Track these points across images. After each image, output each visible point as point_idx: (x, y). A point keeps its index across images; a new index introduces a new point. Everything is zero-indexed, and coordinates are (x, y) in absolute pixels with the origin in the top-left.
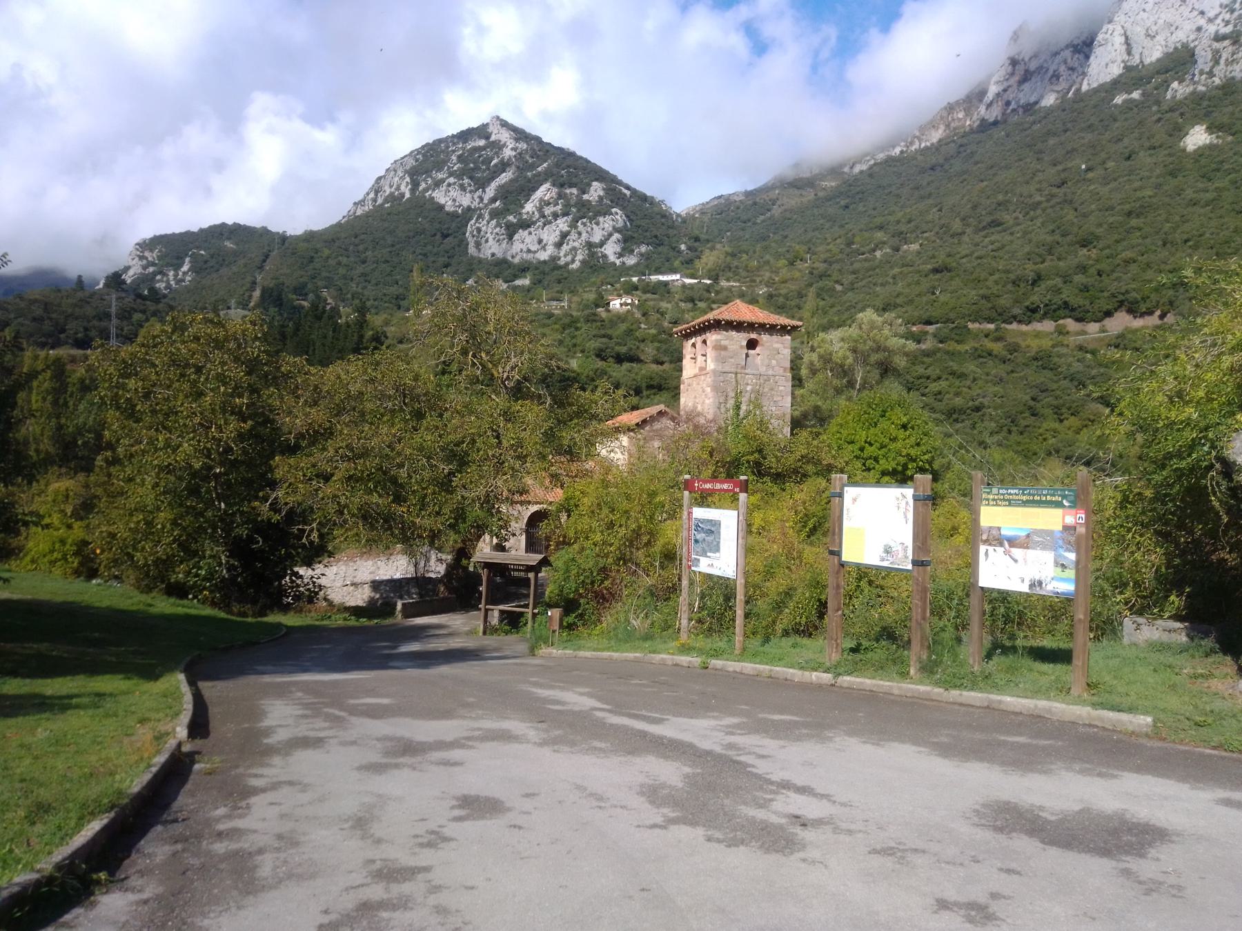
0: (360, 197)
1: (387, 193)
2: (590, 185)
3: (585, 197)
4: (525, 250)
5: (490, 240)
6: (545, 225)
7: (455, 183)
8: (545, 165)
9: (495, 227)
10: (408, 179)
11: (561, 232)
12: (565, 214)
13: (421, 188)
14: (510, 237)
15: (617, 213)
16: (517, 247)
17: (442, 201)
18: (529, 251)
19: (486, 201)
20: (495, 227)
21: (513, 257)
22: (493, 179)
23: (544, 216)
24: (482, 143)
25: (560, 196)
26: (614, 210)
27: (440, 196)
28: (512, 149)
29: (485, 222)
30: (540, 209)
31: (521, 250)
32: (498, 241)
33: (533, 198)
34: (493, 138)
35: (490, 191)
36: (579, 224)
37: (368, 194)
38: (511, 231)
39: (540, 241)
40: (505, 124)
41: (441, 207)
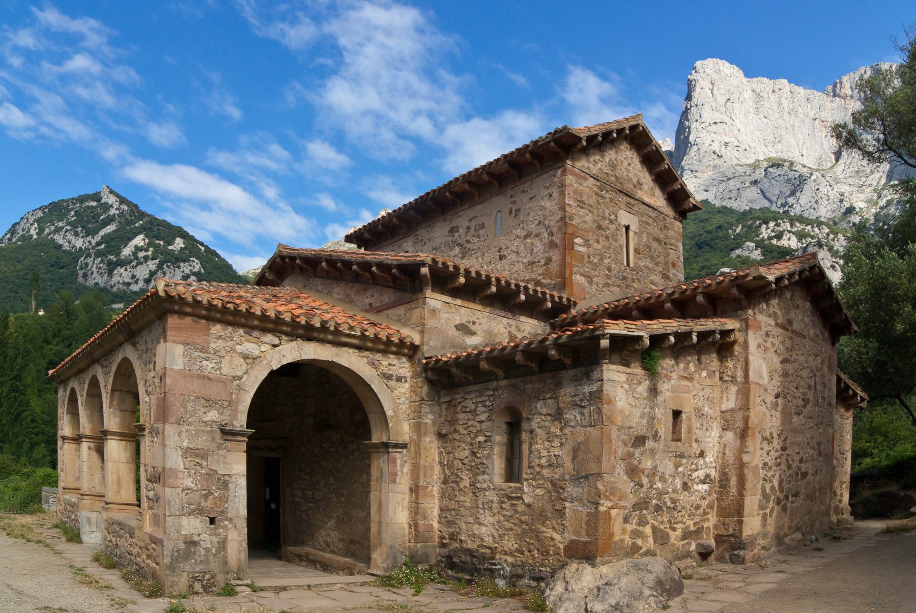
2: (174, 239)
3: (170, 247)
4: (121, 282)
5: (95, 272)
6: (138, 264)
8: (141, 222)
9: (100, 263)
11: (150, 271)
12: (153, 259)
14: (110, 273)
15: (194, 261)
16: (116, 279)
20: (100, 263)
21: (112, 287)
23: (137, 258)
25: (150, 244)
26: (192, 259)
30: (135, 254)
31: (119, 282)
36: (165, 266)
38: (111, 268)
39: (133, 277)
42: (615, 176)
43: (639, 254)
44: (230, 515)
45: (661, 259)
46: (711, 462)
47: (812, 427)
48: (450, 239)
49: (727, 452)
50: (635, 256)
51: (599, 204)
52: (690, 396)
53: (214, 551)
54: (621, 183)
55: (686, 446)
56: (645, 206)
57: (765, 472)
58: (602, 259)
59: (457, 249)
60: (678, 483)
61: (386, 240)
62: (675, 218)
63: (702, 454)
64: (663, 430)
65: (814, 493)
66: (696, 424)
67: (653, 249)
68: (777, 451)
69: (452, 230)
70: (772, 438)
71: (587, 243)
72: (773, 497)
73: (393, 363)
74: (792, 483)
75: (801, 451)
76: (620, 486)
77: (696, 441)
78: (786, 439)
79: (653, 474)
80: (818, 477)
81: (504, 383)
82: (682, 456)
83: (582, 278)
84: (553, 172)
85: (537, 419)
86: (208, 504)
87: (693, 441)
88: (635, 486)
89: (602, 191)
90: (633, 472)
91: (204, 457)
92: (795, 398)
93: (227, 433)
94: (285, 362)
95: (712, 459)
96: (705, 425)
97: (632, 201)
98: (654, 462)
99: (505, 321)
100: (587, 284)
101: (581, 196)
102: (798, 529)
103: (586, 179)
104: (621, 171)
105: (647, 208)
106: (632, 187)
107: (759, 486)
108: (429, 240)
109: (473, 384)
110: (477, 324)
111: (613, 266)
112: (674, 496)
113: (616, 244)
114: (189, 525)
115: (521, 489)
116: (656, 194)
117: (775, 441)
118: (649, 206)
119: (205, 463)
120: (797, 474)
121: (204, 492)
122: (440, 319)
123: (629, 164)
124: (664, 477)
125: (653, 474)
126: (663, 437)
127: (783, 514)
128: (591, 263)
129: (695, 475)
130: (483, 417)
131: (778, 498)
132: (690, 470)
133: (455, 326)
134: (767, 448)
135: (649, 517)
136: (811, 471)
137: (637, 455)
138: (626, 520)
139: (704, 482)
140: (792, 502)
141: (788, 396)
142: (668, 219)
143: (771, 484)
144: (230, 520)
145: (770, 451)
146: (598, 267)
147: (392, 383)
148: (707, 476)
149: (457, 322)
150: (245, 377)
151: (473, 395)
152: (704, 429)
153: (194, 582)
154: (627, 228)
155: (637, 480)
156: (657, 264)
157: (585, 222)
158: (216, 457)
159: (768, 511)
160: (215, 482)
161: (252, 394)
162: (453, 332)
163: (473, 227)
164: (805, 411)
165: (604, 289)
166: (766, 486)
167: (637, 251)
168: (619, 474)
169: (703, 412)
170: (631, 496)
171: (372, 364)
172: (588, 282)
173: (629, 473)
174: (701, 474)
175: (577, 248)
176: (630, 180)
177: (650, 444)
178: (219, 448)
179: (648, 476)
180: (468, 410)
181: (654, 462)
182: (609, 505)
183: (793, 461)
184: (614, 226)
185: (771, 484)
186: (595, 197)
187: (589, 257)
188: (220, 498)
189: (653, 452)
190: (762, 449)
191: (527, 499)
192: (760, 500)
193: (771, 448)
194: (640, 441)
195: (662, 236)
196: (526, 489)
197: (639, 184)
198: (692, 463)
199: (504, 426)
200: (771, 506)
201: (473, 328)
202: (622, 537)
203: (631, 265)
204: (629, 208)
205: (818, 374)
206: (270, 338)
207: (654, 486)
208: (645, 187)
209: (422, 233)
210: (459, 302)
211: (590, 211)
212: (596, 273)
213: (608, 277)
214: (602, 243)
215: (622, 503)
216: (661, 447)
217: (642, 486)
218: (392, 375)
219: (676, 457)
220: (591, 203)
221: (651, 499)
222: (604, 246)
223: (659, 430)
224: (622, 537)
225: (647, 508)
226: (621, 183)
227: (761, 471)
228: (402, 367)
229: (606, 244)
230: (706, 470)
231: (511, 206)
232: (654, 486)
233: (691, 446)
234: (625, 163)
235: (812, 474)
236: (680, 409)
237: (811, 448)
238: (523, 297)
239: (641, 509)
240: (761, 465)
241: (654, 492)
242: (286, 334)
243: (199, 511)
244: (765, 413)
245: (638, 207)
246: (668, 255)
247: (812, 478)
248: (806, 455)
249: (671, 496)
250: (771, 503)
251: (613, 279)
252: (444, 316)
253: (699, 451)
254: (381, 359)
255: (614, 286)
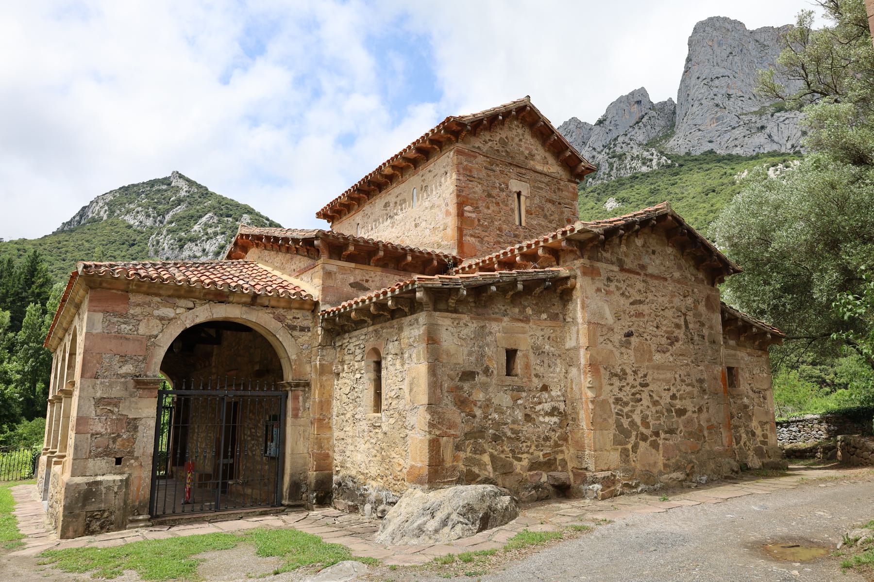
0: (68, 220)
1: (90, 217)
2: (242, 216)
4: (191, 255)
6: (208, 239)
7: (141, 211)
8: (210, 202)
9: (171, 240)
10: (106, 208)
12: (223, 233)
13: (115, 214)
16: (186, 253)
17: (132, 222)
18: (195, 257)
19: (165, 223)
22: (172, 209)
23: (207, 234)
24: (164, 187)
25: (219, 222)
27: (130, 220)
28: (186, 191)
29: (163, 236)
32: (172, 249)
33: (200, 222)
34: (173, 184)
35: (168, 217)
37: (74, 217)
39: (204, 250)
40: (181, 176)
41: (130, 227)
42: (506, 151)
43: (531, 214)
44: (136, 454)
45: (556, 217)
46: (558, 396)
47: (687, 365)
48: (385, 212)
49: (574, 387)
50: (526, 217)
51: (489, 176)
52: (527, 336)
53: (116, 490)
54: (512, 157)
55: (524, 380)
56: (536, 174)
57: (619, 407)
58: (492, 221)
59: (389, 221)
60: (519, 415)
61: (345, 215)
62: (569, 181)
63: (545, 388)
64: (495, 366)
65: (701, 431)
66: (533, 360)
67: (546, 209)
68: (633, 387)
69: (386, 205)
70: (625, 374)
71: (476, 209)
72: (634, 433)
73: (297, 317)
74: (663, 419)
75: (672, 388)
76: (448, 415)
77: (537, 376)
78: (645, 376)
79: (488, 404)
80: (704, 416)
81: (371, 329)
82: (520, 389)
83: (473, 239)
84: (448, 154)
85: (389, 358)
86: (117, 445)
87: (533, 376)
88: (467, 416)
89: (492, 165)
90: (463, 403)
91: (116, 405)
92: (656, 336)
93: (141, 383)
94: (198, 321)
95: (559, 393)
96: (546, 362)
97: (523, 171)
98: (487, 394)
99: (397, 278)
100: (477, 243)
101: (470, 171)
102: (677, 468)
103: (475, 157)
104: (513, 146)
105: (539, 175)
106: (523, 158)
107: (612, 421)
108: (372, 213)
109: (355, 330)
110: (370, 281)
111: (504, 226)
112: (515, 427)
113: (508, 208)
114: (94, 466)
115: (380, 418)
116: (549, 162)
117: (630, 379)
118: (541, 173)
119: (117, 410)
120: (669, 411)
121: (113, 435)
122: (336, 279)
123: (521, 140)
124: (500, 409)
125: (488, 404)
126: (495, 372)
127: (654, 451)
128: (482, 225)
129: (538, 408)
130: (359, 358)
131: (642, 434)
132: (532, 403)
133: (350, 284)
134: (617, 383)
135: (486, 446)
136: (690, 408)
137: (466, 388)
138: (458, 448)
139: (551, 414)
140: (665, 439)
141: (645, 335)
142: (562, 183)
143: (629, 420)
144: (137, 459)
145: (623, 386)
146: (488, 228)
147: (295, 333)
148: (554, 409)
149: (352, 281)
150: (160, 335)
151: (354, 340)
152: (546, 365)
153: (91, 521)
154: (519, 194)
155: (468, 411)
156: (551, 222)
157: (474, 193)
158: (127, 403)
159: (629, 446)
160: (125, 425)
161: (166, 349)
162: (348, 289)
163: (398, 202)
164: (673, 349)
165: (495, 246)
166: (622, 420)
167: (527, 212)
168: (446, 405)
169: (544, 350)
170: (463, 425)
171: (279, 319)
172: (479, 242)
173: (459, 404)
174: (547, 407)
175: (467, 214)
176: (522, 153)
177: (481, 378)
178: (131, 396)
179: (480, 407)
180: (351, 352)
181: (487, 394)
182: (438, 433)
183: (661, 397)
184: (504, 194)
185: (629, 420)
186: (484, 172)
187: (479, 220)
188: (128, 440)
189: (485, 387)
190: (612, 385)
191: (385, 428)
192: (615, 435)
193: (625, 384)
194: (468, 376)
195: (554, 197)
196: (384, 419)
197: (532, 156)
198: (534, 397)
199: (372, 365)
200: (632, 442)
201: (366, 285)
202: (455, 463)
203: (523, 224)
204: (520, 177)
205: (690, 313)
206: (183, 303)
207: (490, 417)
208: (538, 157)
209: (367, 208)
210: (353, 265)
211: (480, 183)
212: (486, 234)
213: (499, 235)
214: (492, 208)
215: (452, 432)
216: (494, 381)
217: (474, 416)
218: (296, 327)
219: (513, 390)
220: (481, 177)
221: (486, 428)
222: (493, 211)
223: (491, 366)
224: (455, 463)
225: (483, 438)
226: (512, 157)
227: (613, 406)
228: (303, 319)
229: (496, 208)
230: (553, 403)
231: (422, 183)
232: (490, 417)
233: (531, 381)
234: (517, 139)
235: (694, 412)
236: (514, 347)
237: (688, 385)
238: (409, 258)
239: (475, 438)
240: (611, 400)
241: (490, 422)
242: (200, 299)
243: (106, 453)
244: (612, 351)
245: (530, 175)
246: (562, 213)
247: (695, 415)
248: (681, 392)
249: (511, 426)
250: (633, 438)
251: (504, 238)
252: (340, 276)
253: (541, 386)
254: (285, 314)
255: (505, 243)
